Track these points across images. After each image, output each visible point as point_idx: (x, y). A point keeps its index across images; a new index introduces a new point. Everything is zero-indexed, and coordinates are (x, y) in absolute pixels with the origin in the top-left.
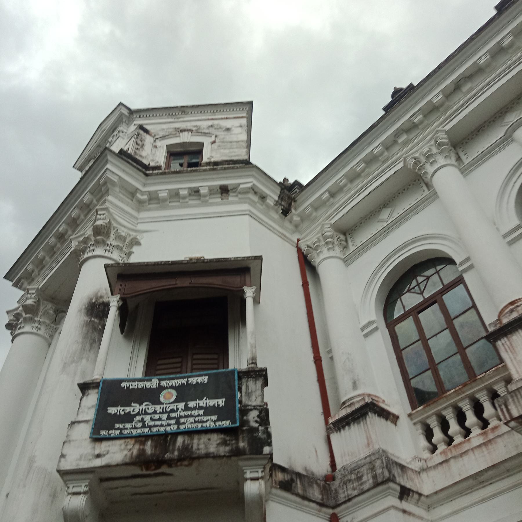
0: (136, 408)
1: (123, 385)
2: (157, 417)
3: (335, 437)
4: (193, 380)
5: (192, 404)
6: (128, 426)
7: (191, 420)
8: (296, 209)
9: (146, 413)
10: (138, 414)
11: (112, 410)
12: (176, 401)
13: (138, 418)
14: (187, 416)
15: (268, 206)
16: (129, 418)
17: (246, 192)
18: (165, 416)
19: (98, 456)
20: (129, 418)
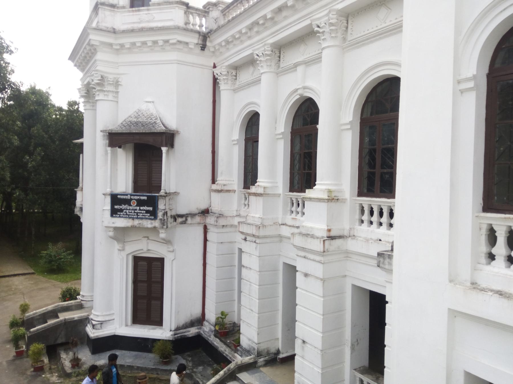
0: (123, 207)
1: (119, 196)
2: (130, 211)
4: (142, 198)
5: (141, 208)
6: (122, 213)
7: (141, 214)
8: (211, 41)
9: (127, 209)
10: (124, 209)
11: (116, 207)
12: (136, 206)
13: (125, 211)
14: (140, 213)
15: (191, 49)
16: (121, 210)
18: (133, 211)
19: (113, 223)
20: (121, 210)
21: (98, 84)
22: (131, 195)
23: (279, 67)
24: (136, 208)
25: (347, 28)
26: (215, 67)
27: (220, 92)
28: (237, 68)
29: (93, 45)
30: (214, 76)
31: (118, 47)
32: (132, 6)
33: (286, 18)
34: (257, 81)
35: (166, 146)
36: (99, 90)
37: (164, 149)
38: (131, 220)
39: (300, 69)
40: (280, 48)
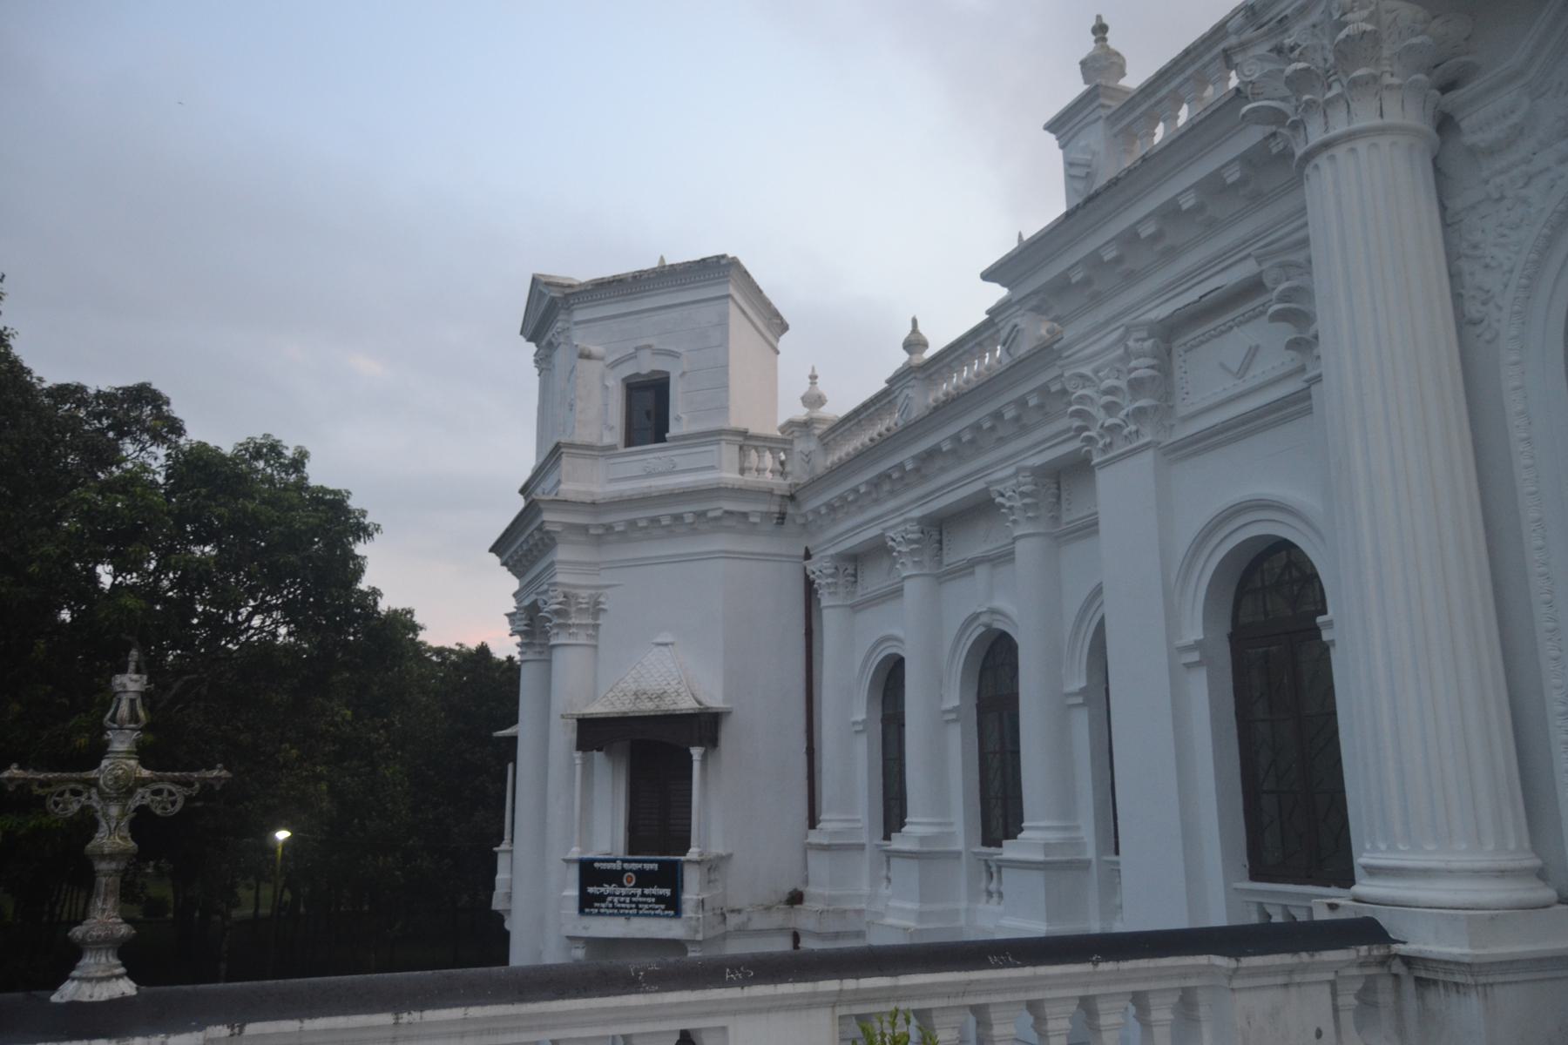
0: (607, 889)
1: (597, 865)
3: (811, 854)
4: (648, 866)
5: (647, 891)
11: (591, 890)
17: (716, 519)
20: (602, 898)
21: (557, 613)
22: (624, 861)
23: (940, 562)
24: (633, 891)
25: (1059, 497)
26: (808, 556)
27: (820, 611)
28: (855, 562)
29: (548, 532)
30: (807, 577)
31: (600, 531)
32: (629, 442)
33: (943, 470)
34: (897, 593)
35: (700, 744)
36: (559, 626)
37: (696, 752)
38: (622, 920)
39: (982, 572)
40: (940, 527)
